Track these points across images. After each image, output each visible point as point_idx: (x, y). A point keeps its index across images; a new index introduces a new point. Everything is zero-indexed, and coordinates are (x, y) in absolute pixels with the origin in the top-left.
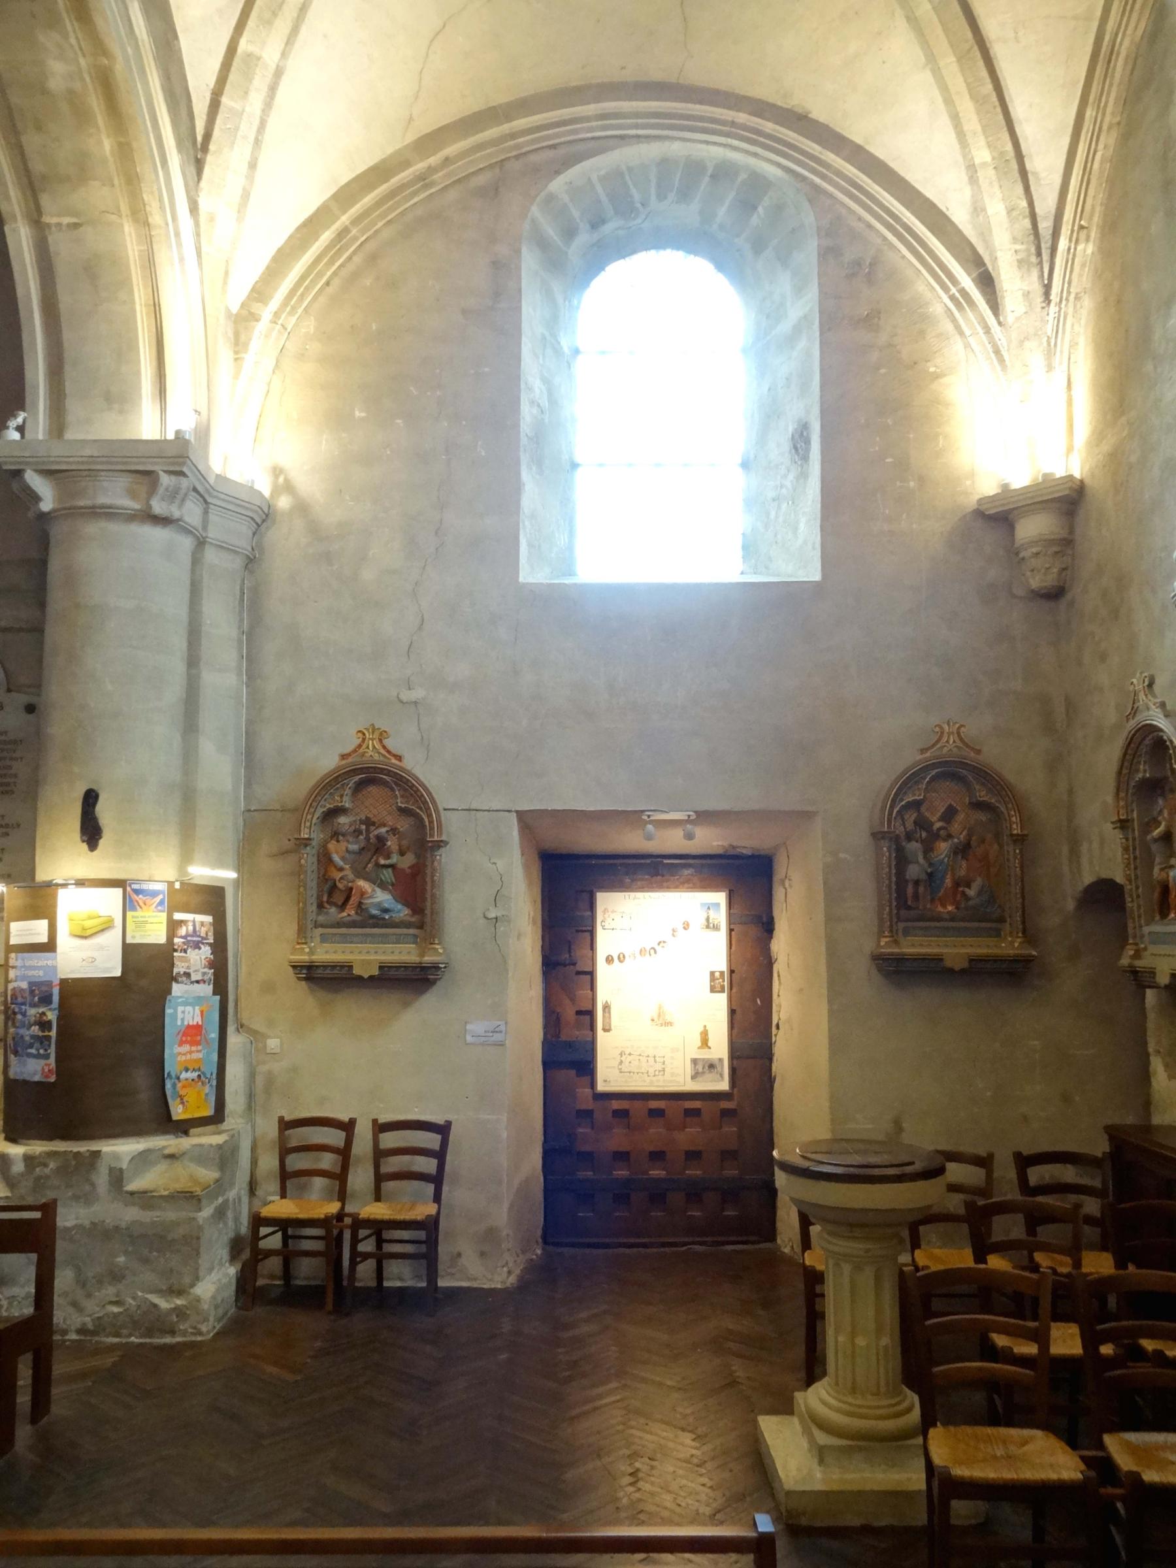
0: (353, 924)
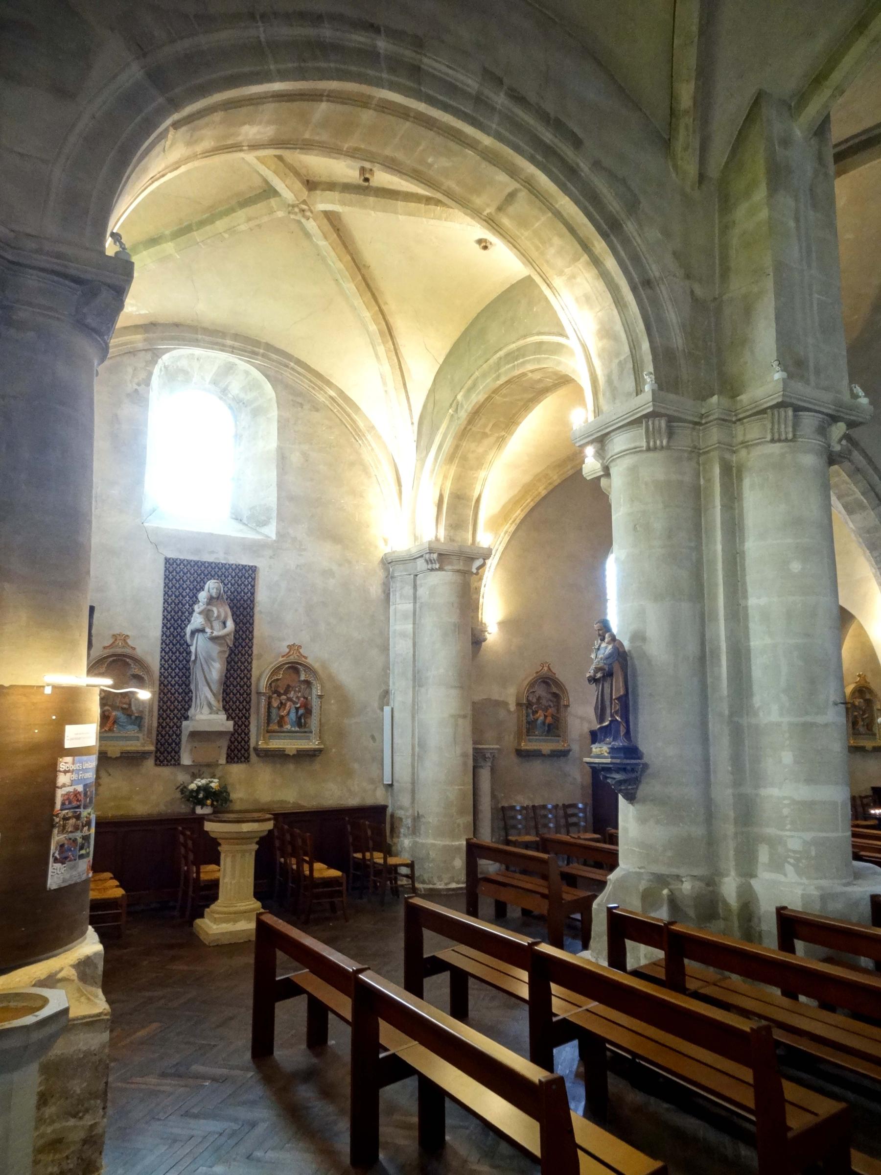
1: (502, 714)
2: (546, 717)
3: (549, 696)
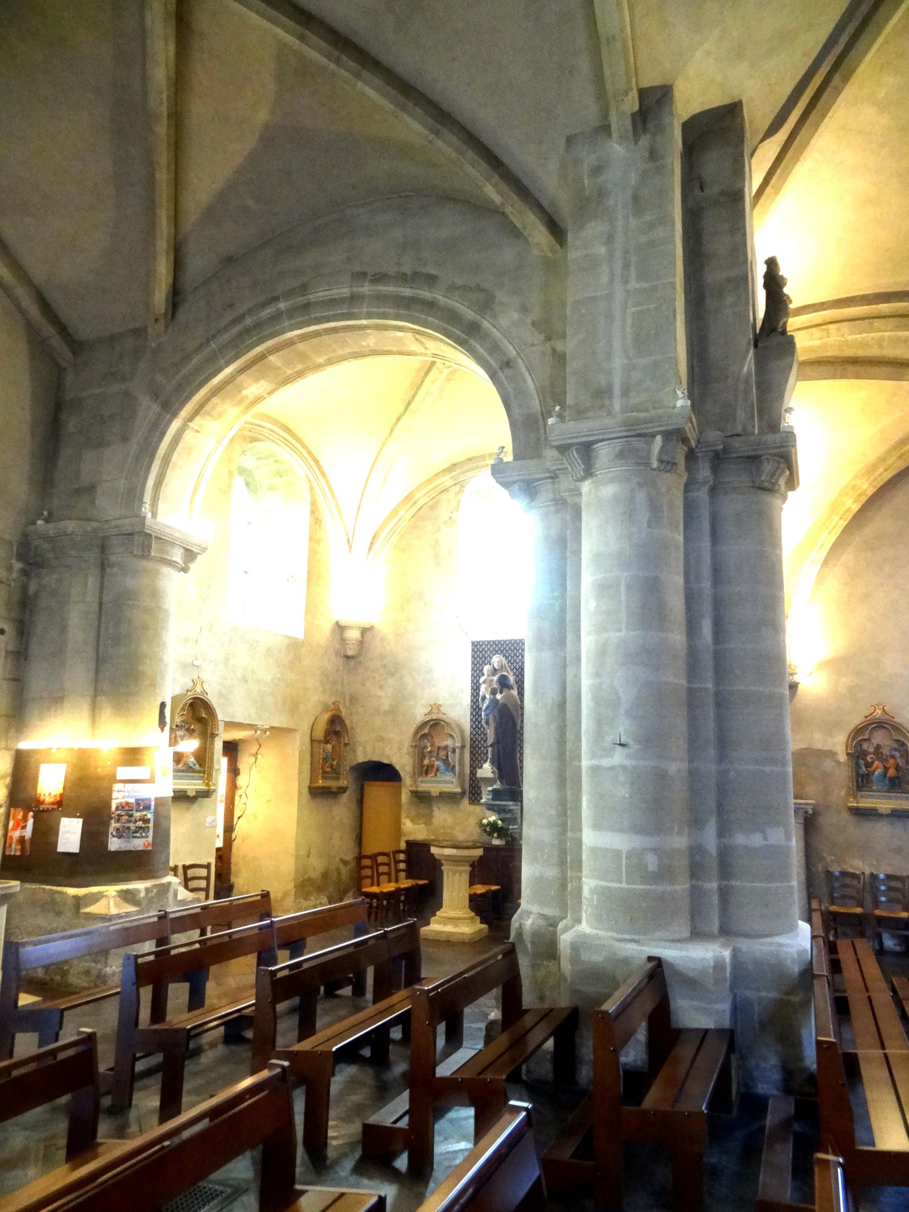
0: (183, 771)
1: (828, 764)
2: (886, 769)
3: (895, 745)
